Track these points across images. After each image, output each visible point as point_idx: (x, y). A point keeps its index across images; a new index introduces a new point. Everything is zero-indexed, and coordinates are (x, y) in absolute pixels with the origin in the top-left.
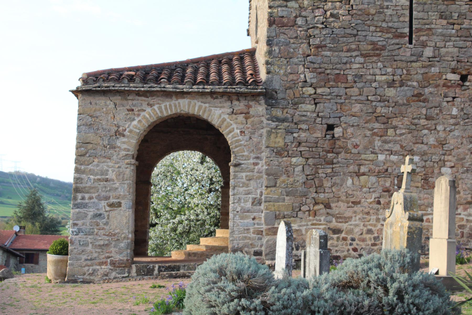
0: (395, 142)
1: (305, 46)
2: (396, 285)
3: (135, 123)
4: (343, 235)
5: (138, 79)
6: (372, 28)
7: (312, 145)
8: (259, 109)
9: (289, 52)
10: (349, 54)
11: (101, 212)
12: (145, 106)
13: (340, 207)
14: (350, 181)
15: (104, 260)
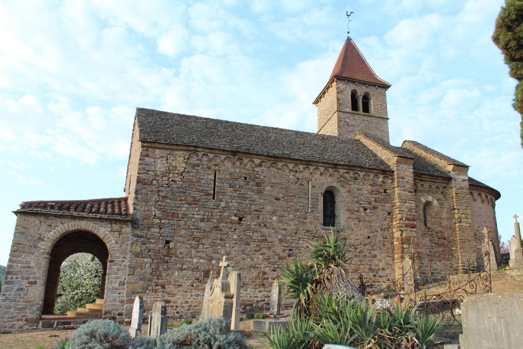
0: (203, 252)
1: (156, 196)
2: (217, 343)
3: (52, 233)
4: (171, 304)
5: (56, 208)
6: (194, 190)
7: (156, 252)
8: (128, 229)
9: (147, 199)
10: (180, 202)
11: (23, 287)
12: (59, 224)
13: (170, 288)
14: (177, 273)
15: (21, 318)
